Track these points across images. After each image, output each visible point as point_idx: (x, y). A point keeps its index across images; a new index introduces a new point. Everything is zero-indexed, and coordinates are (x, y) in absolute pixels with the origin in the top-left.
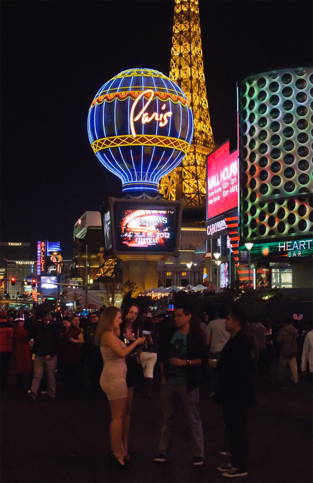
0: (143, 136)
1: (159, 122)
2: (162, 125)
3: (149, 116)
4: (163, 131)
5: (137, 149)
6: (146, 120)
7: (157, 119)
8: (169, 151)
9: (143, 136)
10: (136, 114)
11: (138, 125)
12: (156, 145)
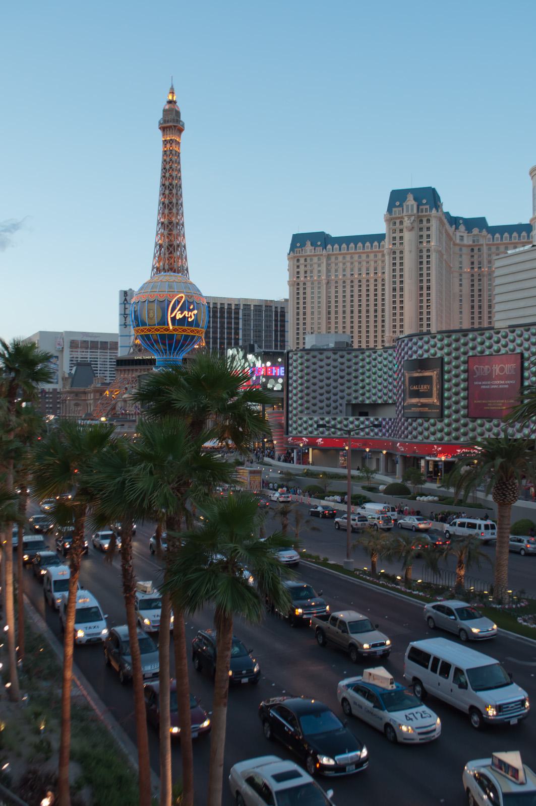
0: (176, 327)
1: (188, 317)
2: (190, 320)
3: (182, 314)
4: (190, 324)
5: (171, 337)
6: (179, 316)
7: (187, 316)
8: (193, 337)
9: (176, 327)
10: (171, 314)
11: (173, 319)
12: (185, 333)
